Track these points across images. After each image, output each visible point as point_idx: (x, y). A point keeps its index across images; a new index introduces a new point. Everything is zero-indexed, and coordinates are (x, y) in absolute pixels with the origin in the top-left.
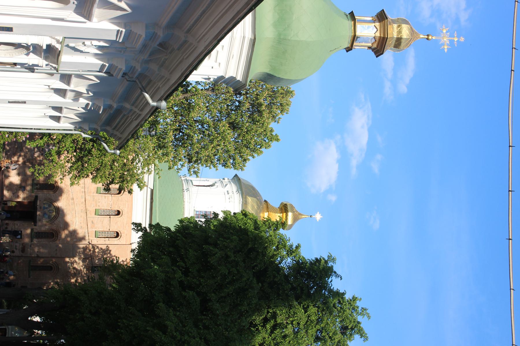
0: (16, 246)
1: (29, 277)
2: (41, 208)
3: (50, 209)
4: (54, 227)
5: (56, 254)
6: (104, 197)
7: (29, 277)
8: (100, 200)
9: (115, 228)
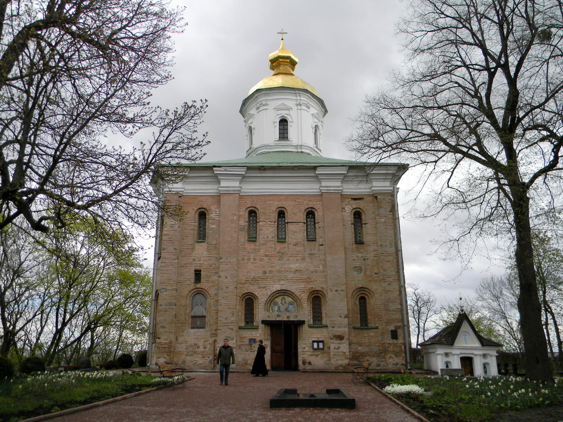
0: (334, 349)
1: (377, 328)
2: (278, 316)
3: (280, 302)
4: (304, 297)
5: (342, 291)
6: (261, 232)
7: (377, 328)
8: (266, 237)
9: (302, 217)
